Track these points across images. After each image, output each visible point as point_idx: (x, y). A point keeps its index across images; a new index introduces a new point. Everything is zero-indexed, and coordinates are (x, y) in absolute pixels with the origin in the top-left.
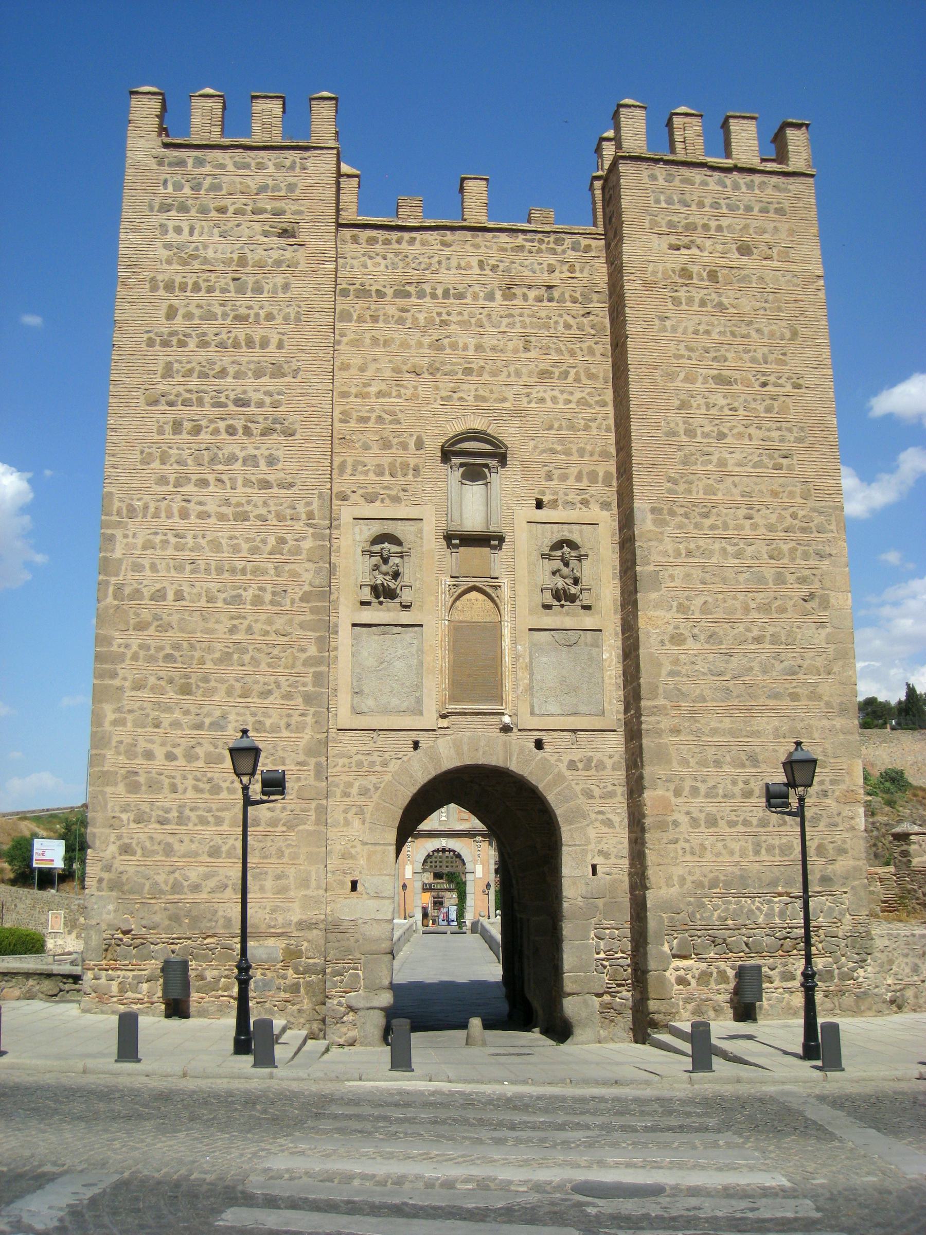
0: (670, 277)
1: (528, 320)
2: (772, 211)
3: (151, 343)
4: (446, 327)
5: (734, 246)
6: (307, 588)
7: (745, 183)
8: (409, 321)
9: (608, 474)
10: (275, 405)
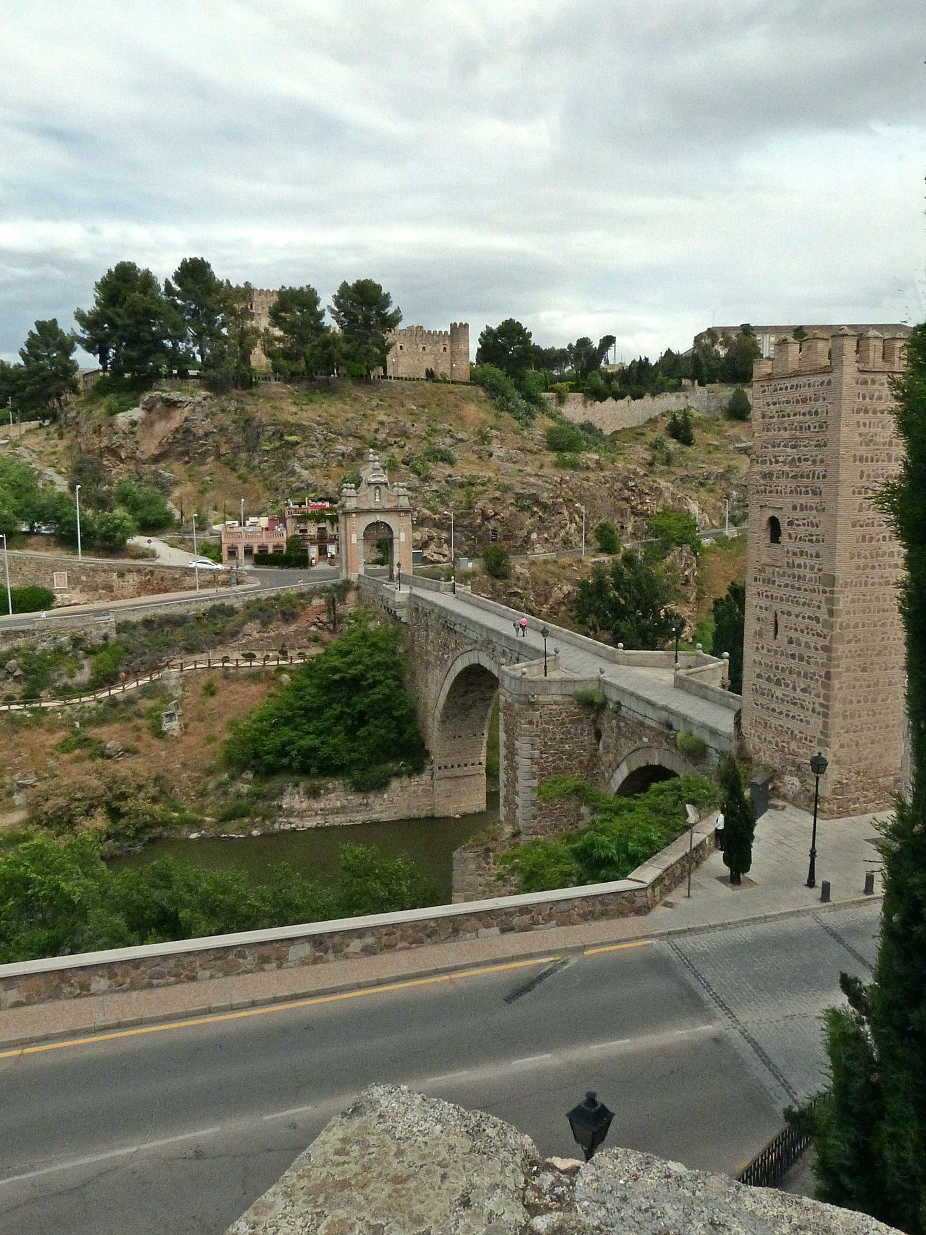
3: (854, 493)
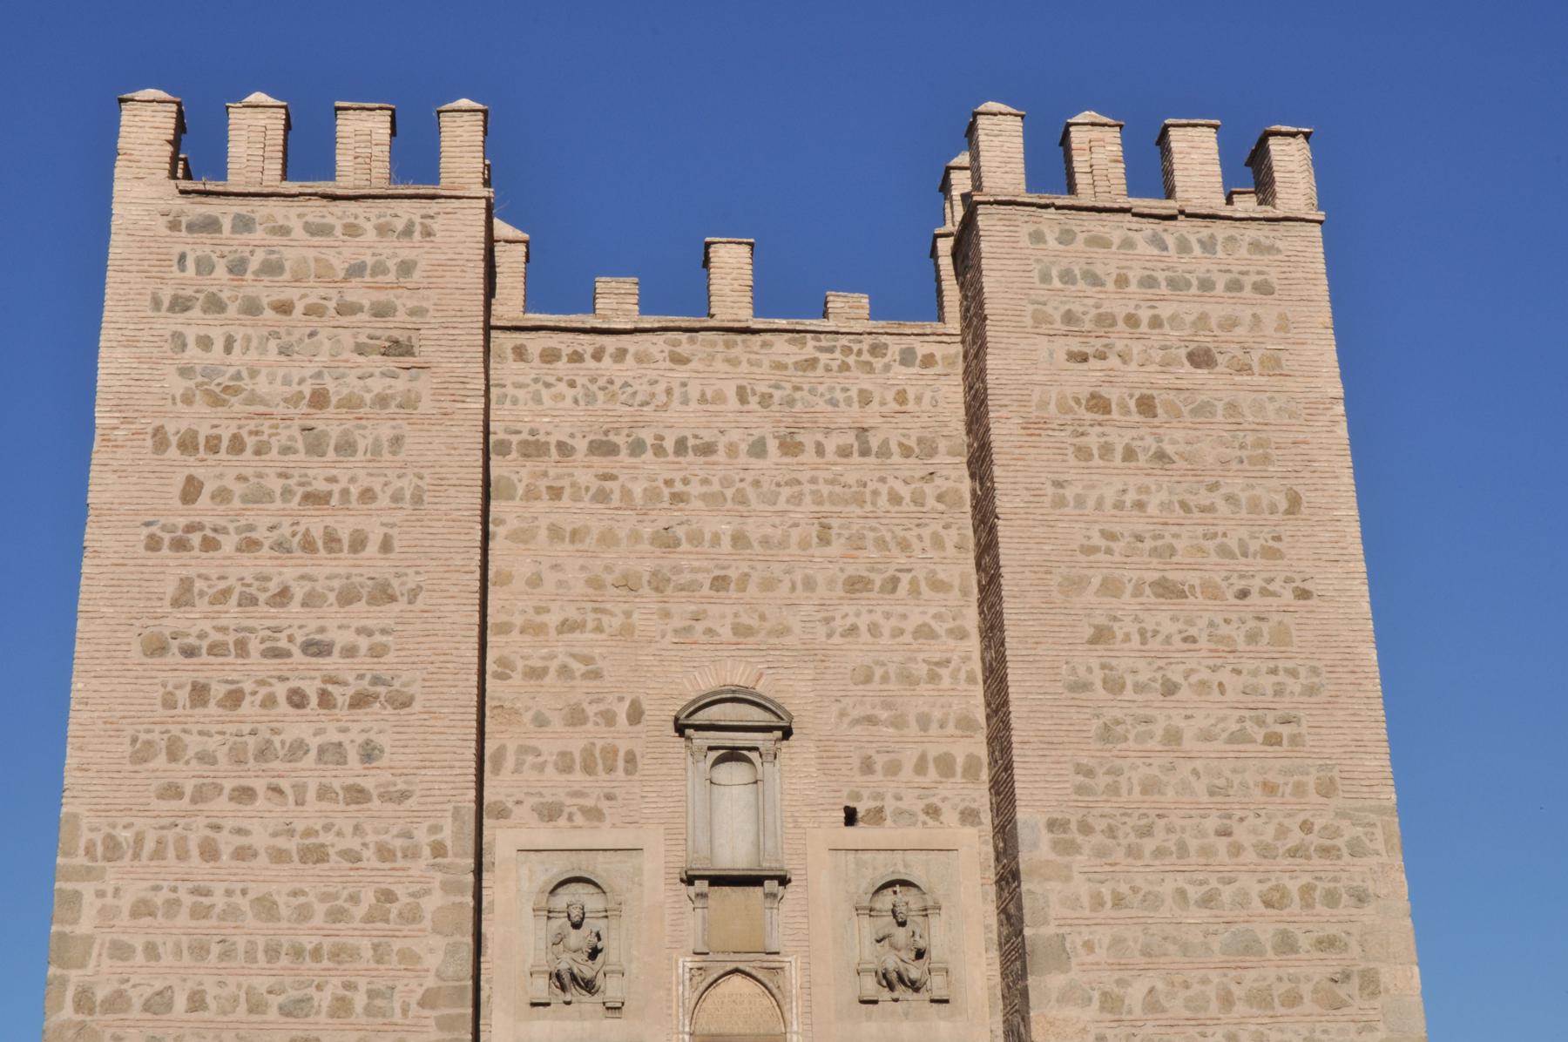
0: (1071, 410)
1: (825, 490)
2: (1248, 288)
3: (153, 544)
4: (682, 505)
5: (1183, 352)
6: (431, 982)
7: (1199, 241)
8: (616, 496)
9: (972, 762)
10: (377, 652)
